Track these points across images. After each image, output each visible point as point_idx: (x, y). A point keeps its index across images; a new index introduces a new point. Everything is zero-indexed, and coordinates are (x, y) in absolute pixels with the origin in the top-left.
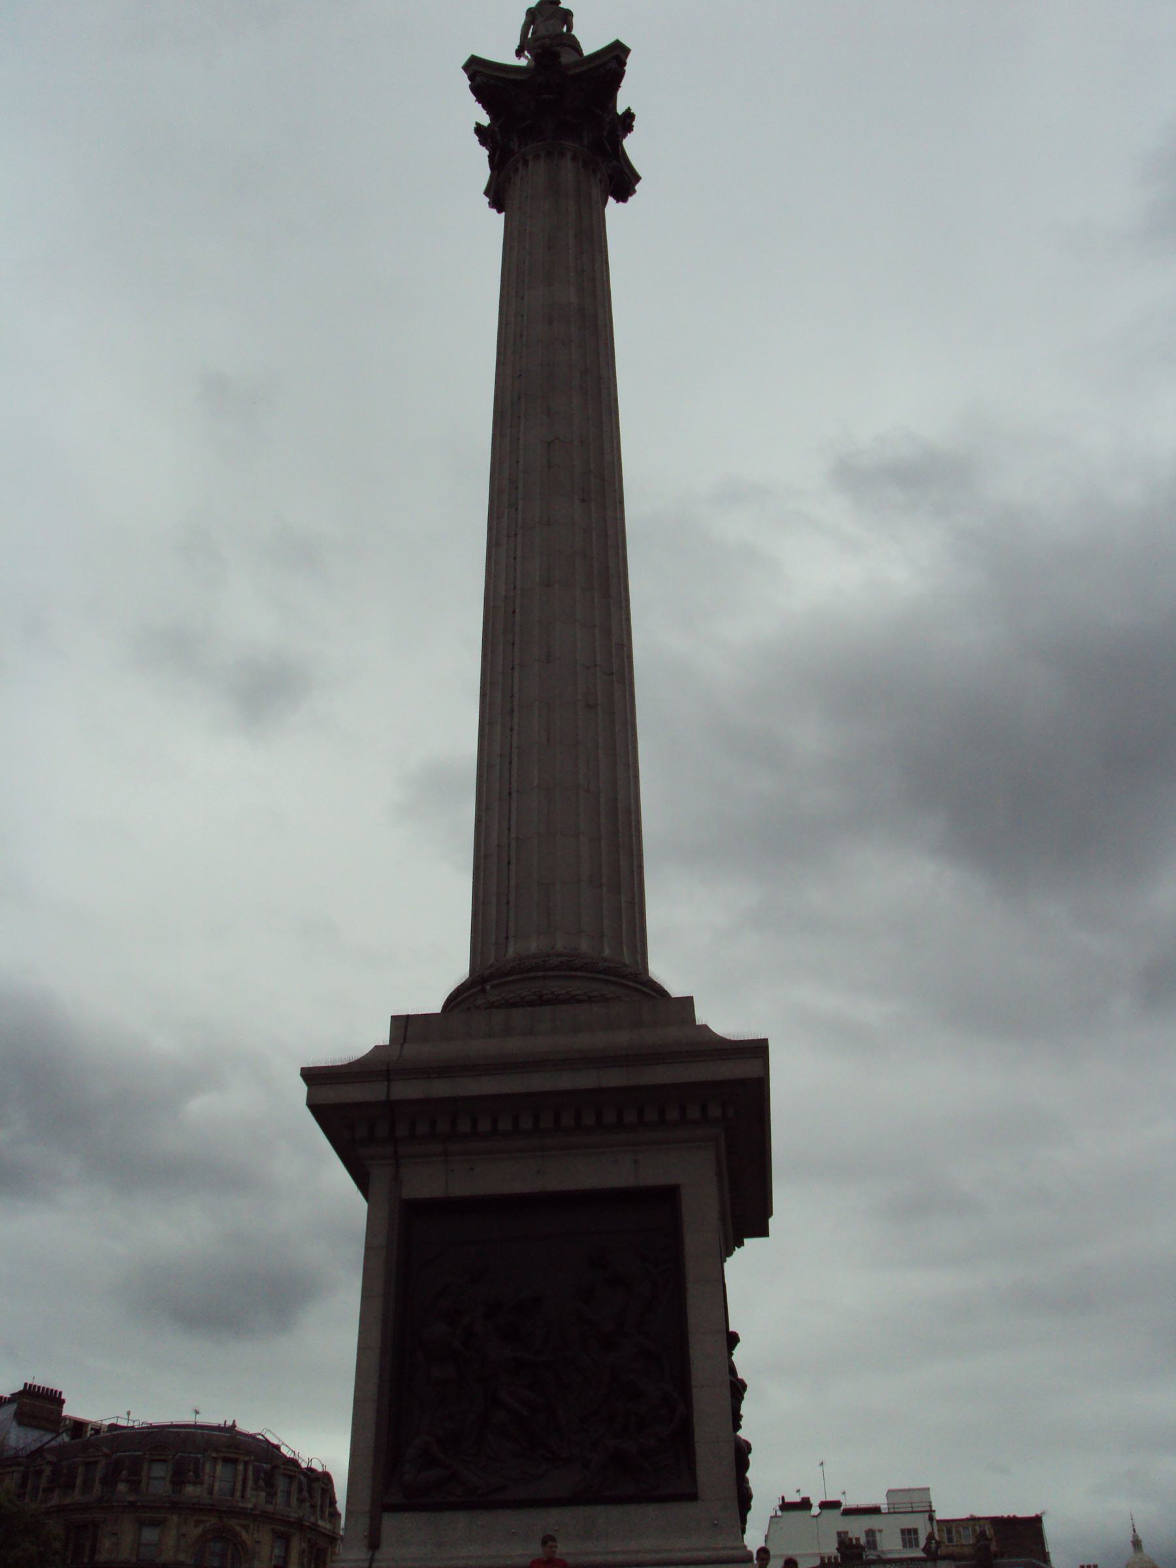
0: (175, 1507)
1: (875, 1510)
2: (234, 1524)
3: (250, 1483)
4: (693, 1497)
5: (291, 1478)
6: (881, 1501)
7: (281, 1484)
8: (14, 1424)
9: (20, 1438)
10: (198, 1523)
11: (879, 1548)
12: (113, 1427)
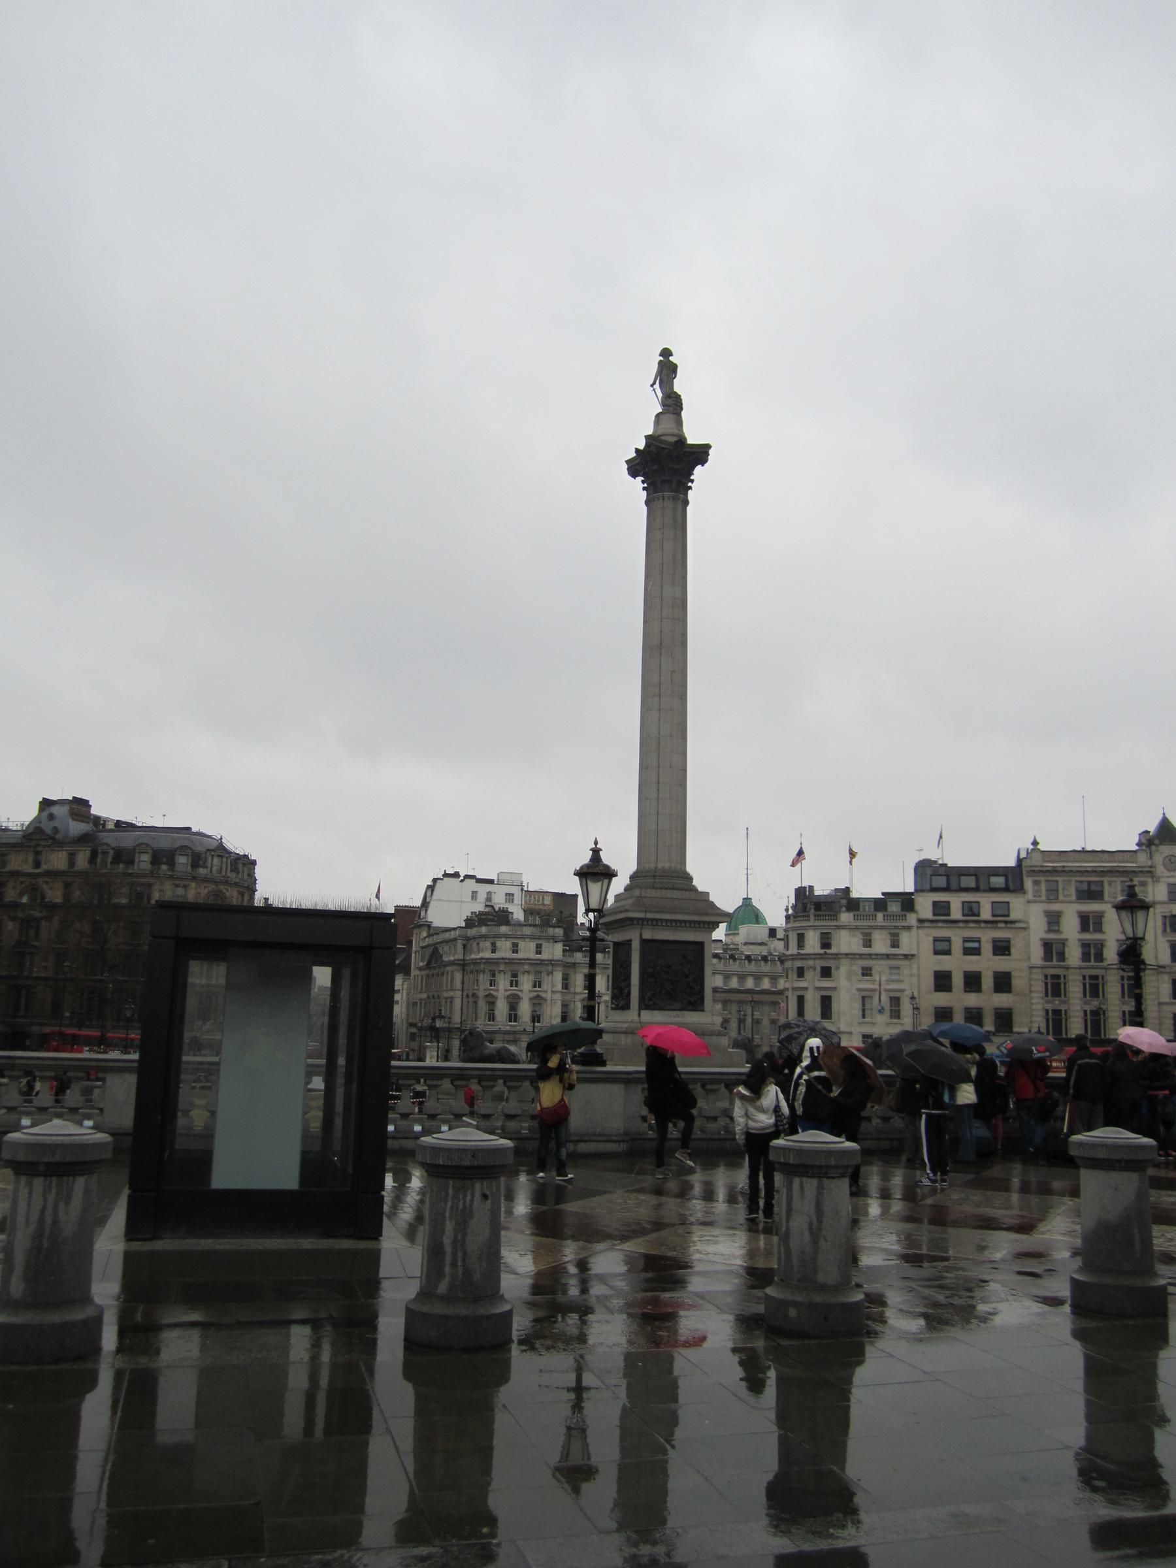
0: (194, 878)
1: (491, 882)
2: (222, 887)
3: (229, 868)
4: (704, 1011)
5: (244, 864)
6: (495, 877)
7: (241, 867)
8: (70, 820)
9: (77, 828)
10: (205, 888)
11: (493, 901)
12: (118, 824)
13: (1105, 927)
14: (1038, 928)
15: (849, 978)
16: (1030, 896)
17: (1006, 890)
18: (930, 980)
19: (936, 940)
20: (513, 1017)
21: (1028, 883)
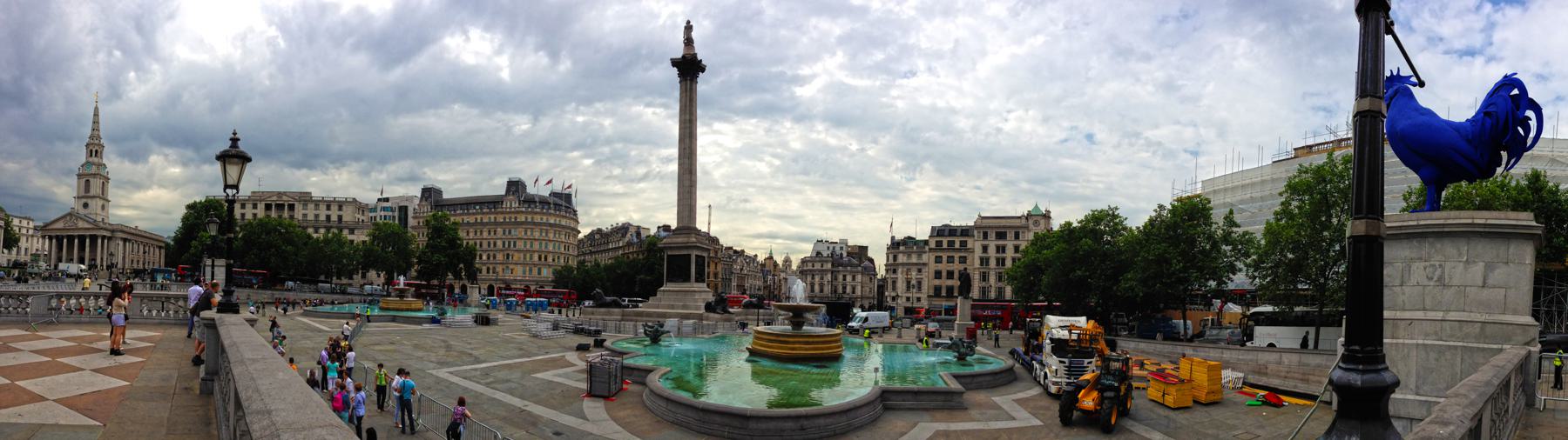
13: (1007, 251)
14: (978, 252)
15: (902, 273)
16: (976, 238)
17: (967, 235)
18: (932, 275)
19: (936, 257)
20: (822, 291)
21: (975, 232)
